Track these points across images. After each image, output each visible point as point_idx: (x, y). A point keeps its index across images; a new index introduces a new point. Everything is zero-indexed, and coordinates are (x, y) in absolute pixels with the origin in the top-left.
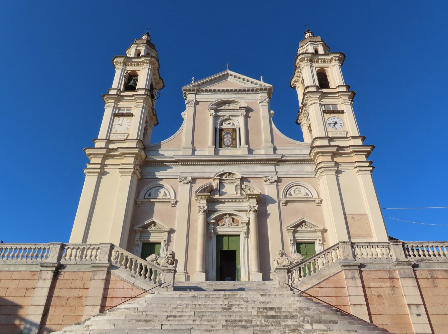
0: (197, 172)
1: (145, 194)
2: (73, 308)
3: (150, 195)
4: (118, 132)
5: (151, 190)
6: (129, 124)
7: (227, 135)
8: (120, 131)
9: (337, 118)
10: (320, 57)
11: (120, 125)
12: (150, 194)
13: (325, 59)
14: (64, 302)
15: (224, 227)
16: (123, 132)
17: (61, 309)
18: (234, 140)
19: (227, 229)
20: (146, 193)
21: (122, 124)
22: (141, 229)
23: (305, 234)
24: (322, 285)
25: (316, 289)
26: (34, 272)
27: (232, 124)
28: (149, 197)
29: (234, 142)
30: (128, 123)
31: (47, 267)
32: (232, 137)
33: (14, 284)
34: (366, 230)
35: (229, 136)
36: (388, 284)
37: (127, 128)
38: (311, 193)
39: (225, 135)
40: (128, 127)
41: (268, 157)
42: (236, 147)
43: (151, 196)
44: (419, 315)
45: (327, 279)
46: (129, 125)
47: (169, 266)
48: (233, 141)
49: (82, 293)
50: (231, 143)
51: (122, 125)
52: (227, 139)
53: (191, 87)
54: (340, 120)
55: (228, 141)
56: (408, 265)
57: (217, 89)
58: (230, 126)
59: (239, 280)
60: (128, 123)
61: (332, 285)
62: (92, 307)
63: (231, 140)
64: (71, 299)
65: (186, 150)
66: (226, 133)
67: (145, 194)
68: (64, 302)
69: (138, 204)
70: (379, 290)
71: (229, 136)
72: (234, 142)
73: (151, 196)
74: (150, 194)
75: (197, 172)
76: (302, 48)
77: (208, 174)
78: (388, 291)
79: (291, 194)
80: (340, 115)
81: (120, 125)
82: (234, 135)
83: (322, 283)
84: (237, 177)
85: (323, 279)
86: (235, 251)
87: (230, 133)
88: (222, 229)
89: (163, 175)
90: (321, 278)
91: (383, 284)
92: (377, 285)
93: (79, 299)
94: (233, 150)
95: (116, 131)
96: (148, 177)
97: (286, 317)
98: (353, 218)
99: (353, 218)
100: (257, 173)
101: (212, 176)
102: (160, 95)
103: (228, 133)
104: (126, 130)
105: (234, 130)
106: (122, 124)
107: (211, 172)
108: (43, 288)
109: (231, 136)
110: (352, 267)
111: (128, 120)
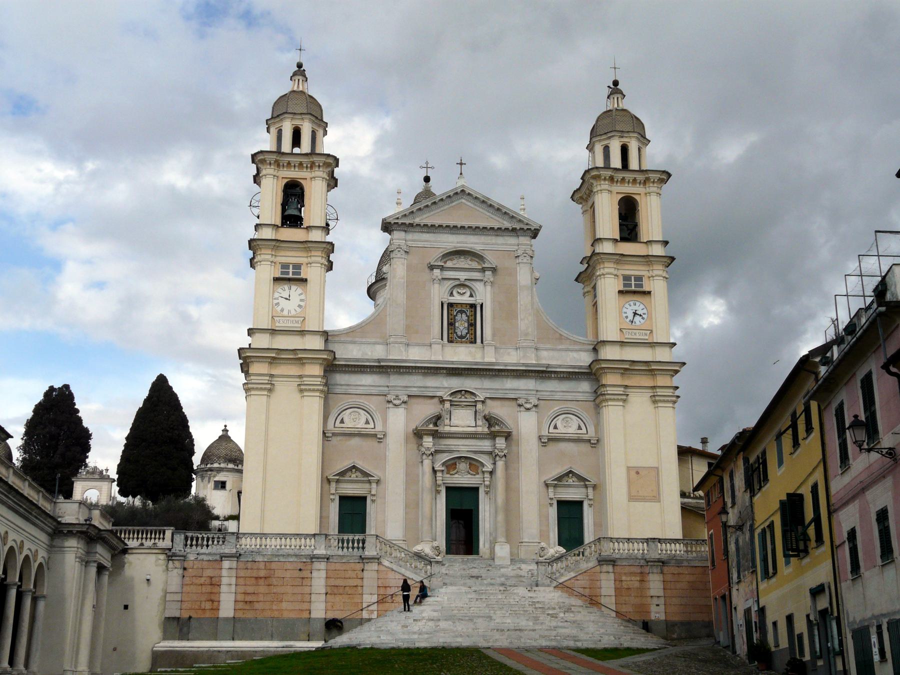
0: (414, 387)
1: (336, 420)
2: (351, 596)
3: (342, 422)
4: (285, 313)
5: (344, 412)
6: (303, 297)
7: (459, 315)
8: (289, 311)
9: (639, 303)
10: (628, 175)
11: (286, 299)
12: (342, 419)
13: (635, 178)
14: (341, 591)
15: (456, 476)
16: (293, 313)
17: (340, 597)
18: (472, 325)
19: (462, 479)
20: (337, 418)
21: (289, 296)
22: (337, 478)
23: (571, 490)
24: (578, 578)
25: (572, 581)
26: (304, 562)
27: (468, 294)
28: (342, 425)
29: (472, 330)
30: (300, 295)
31: (318, 558)
32: (468, 320)
33: (288, 574)
34: (652, 491)
35: (464, 316)
36: (638, 578)
37: (300, 306)
38: (585, 426)
39: (456, 315)
40: (302, 304)
41: (526, 366)
42: (475, 343)
43: (344, 423)
44: (658, 605)
45: (585, 572)
46: (301, 300)
47: (436, 557)
48: (470, 328)
49: (359, 582)
50: (467, 331)
51: (289, 300)
52: (462, 326)
53: (398, 218)
54: (644, 307)
55: (461, 328)
56: (658, 562)
57: (444, 226)
58: (466, 299)
59: (477, 553)
60: (300, 295)
61: (587, 578)
62: (370, 596)
63: (466, 325)
64: (347, 588)
65: (396, 345)
66: (459, 311)
67: (336, 420)
68: (341, 591)
69: (328, 437)
70: (629, 583)
71: (464, 316)
72: (472, 330)
73: (344, 423)
74: (342, 419)
75: (414, 387)
76: (598, 138)
77: (431, 390)
78: (637, 584)
79: (555, 427)
80: (645, 299)
81: (286, 299)
82: (472, 316)
83: (579, 577)
84: (478, 399)
85: (580, 572)
86: (471, 510)
87: (464, 312)
88: (455, 479)
89: (362, 388)
90: (578, 571)
91: (633, 578)
92: (629, 579)
93: (355, 588)
94: (470, 349)
95: (282, 310)
96: (338, 391)
97: (549, 608)
98: (638, 473)
99: (638, 473)
100: (507, 392)
101: (439, 394)
102: (337, 219)
103: (461, 312)
104: (299, 310)
105: (473, 306)
106: (289, 296)
107: (436, 387)
108: (320, 578)
109: (467, 318)
110: (609, 563)
111: (300, 291)
